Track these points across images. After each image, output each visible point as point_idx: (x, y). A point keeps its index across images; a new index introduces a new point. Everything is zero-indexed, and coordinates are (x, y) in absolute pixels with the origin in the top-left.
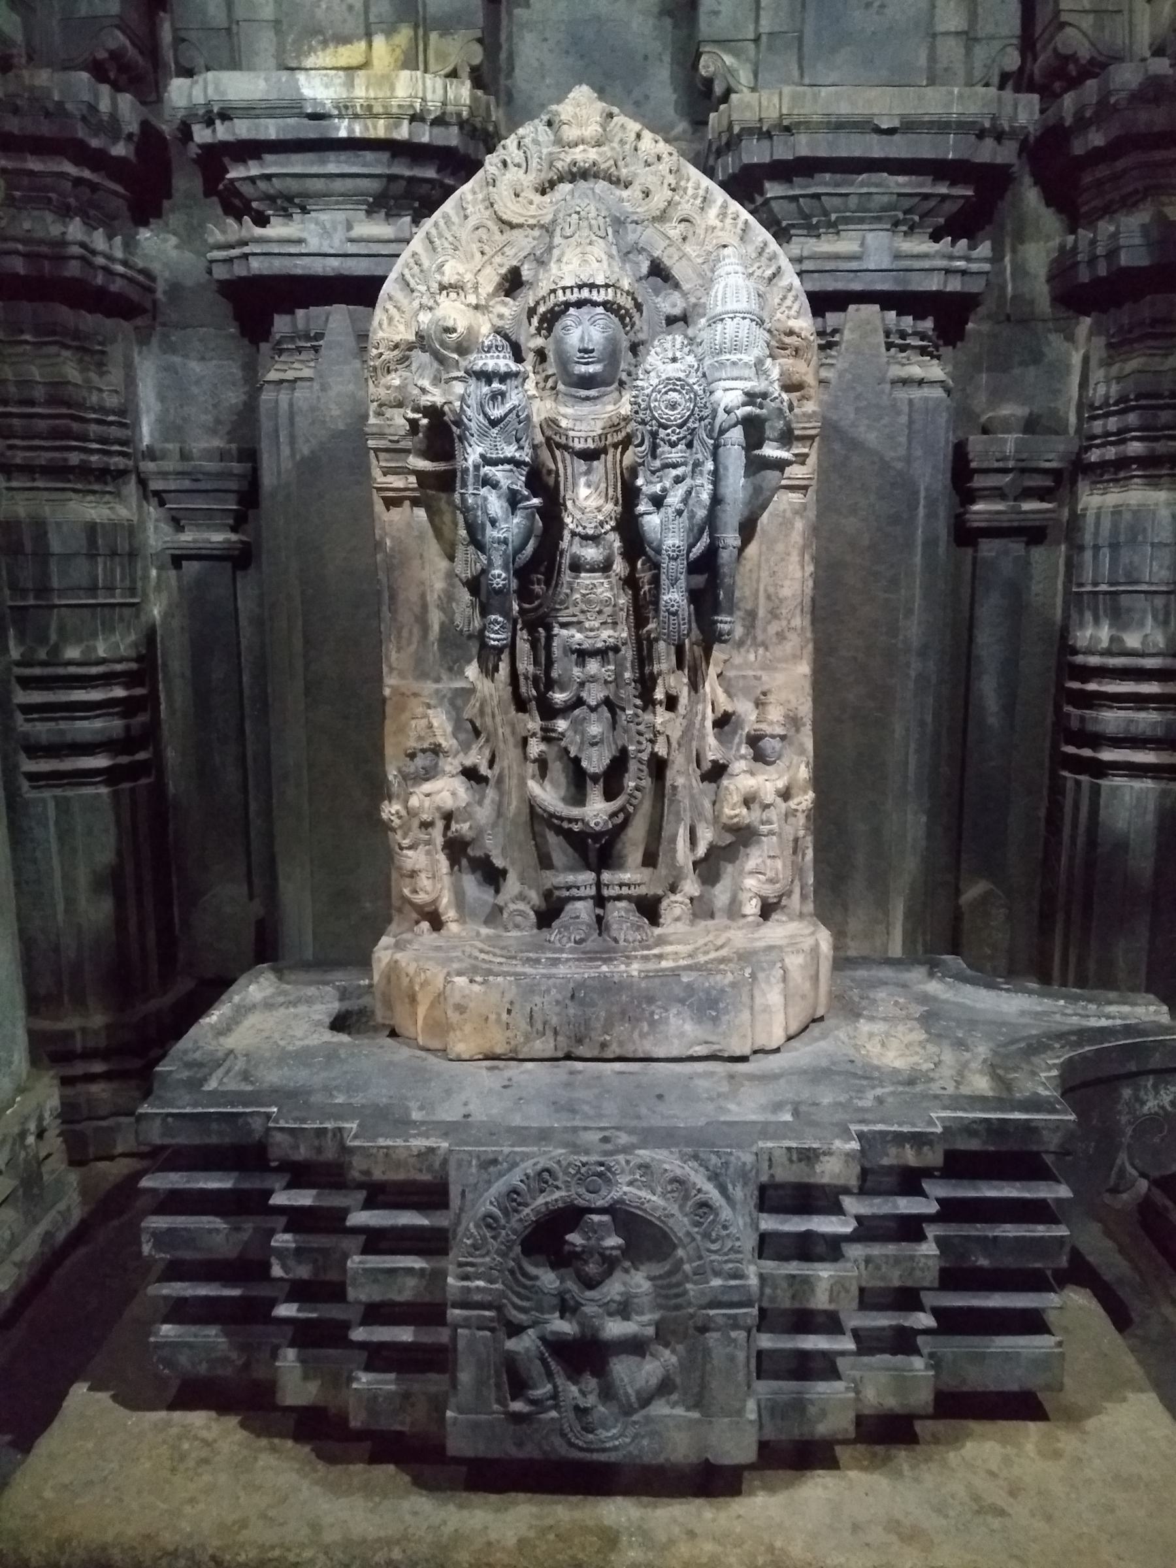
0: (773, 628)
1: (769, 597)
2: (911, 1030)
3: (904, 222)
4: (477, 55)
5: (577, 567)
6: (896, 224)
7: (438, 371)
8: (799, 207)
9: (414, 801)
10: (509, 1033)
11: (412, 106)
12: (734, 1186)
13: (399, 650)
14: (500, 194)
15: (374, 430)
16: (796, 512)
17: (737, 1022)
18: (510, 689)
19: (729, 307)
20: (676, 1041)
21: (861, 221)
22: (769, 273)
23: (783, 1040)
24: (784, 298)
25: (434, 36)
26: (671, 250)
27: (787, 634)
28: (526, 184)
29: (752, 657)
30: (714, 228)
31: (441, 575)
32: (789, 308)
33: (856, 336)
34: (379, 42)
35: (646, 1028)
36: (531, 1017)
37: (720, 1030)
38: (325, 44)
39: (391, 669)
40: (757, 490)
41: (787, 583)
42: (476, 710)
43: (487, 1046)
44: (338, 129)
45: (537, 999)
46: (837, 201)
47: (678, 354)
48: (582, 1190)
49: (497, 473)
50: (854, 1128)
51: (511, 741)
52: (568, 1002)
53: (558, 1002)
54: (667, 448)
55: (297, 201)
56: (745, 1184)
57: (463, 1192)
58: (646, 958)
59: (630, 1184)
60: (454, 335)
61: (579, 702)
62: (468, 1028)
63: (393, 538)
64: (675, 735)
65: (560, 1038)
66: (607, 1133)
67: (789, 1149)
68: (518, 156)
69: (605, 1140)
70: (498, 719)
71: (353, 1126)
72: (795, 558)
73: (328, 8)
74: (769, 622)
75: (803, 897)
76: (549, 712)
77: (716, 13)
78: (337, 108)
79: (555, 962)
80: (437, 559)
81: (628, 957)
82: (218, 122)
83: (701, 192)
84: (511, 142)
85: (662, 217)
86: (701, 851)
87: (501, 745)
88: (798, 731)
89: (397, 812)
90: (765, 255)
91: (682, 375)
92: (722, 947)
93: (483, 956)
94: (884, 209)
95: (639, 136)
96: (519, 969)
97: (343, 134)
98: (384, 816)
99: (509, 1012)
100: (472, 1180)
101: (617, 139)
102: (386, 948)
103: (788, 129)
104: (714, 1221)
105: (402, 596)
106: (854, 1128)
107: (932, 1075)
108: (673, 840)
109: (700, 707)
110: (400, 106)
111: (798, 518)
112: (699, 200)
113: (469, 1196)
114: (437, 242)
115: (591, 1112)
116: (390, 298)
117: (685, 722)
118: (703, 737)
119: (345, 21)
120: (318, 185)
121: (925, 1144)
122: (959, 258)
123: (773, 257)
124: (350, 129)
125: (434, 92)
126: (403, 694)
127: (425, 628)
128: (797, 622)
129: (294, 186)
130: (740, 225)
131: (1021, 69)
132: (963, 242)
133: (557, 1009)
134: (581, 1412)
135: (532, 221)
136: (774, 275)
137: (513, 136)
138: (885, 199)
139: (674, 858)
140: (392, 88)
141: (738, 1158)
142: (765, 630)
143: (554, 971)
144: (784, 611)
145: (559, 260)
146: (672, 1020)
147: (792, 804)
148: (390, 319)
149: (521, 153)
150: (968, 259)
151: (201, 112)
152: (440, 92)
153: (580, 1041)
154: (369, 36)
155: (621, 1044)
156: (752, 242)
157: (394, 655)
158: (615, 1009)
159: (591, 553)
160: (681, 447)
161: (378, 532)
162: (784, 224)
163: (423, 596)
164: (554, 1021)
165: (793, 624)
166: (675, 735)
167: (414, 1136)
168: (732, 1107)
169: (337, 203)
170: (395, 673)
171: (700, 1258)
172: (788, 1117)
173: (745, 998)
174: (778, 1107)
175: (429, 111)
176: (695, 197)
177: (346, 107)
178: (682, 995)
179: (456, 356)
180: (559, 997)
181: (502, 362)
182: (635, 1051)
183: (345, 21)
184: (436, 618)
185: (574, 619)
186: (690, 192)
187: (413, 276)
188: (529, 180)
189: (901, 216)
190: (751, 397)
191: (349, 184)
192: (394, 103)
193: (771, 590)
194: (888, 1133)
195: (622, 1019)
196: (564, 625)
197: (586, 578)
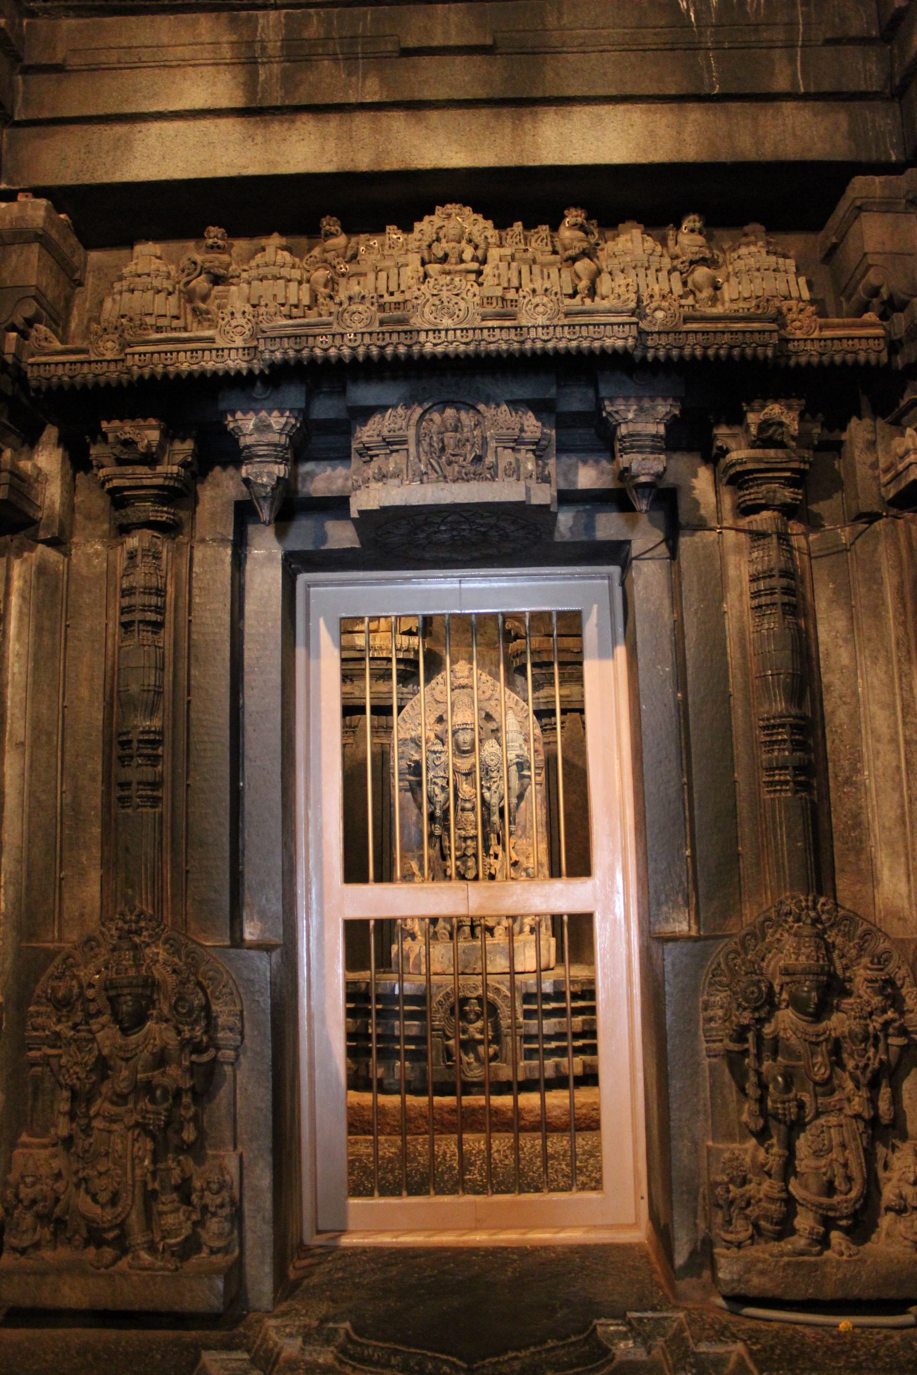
5: (463, 810)
40: (522, 785)
49: (438, 781)
64: (498, 868)
85: (489, 699)
103: (539, 652)
134: (469, 1064)
153: (466, 967)
159: (468, 805)
166: (498, 868)
181: (439, 748)
190: (518, 756)
197: (466, 813)
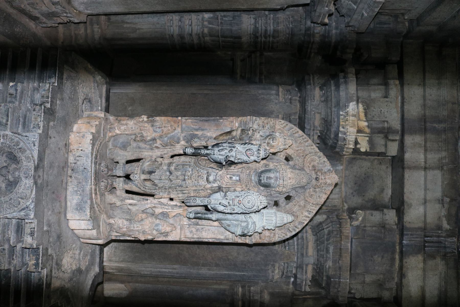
0: (194, 230)
1: (202, 228)
2: (76, 265)
3: (317, 267)
4: (363, 150)
6: (317, 265)
7: (264, 137)
8: (322, 238)
9: (146, 125)
10: (76, 150)
11: (348, 132)
12: (24, 212)
13: (192, 122)
14: (312, 156)
15: (252, 118)
16: (226, 237)
17: (76, 216)
18: (177, 153)
19: (278, 219)
20: (71, 198)
21: (318, 256)
22: (291, 229)
23: (71, 228)
24: (284, 234)
25: (367, 138)
26: (297, 202)
27: (192, 234)
28: (314, 163)
29: (185, 223)
30: (302, 214)
31: (211, 135)
32: (281, 235)
33: (286, 254)
34: (366, 124)
35: (75, 189)
36: (80, 156)
37: (74, 211)
38: (365, 109)
39: (186, 120)
41: (206, 234)
42: (172, 143)
43: (73, 144)
44: (342, 112)
45: (85, 158)
46: (322, 248)
47: (262, 204)
48: (24, 170)
50: (41, 247)
51: (162, 153)
52: (83, 167)
53: (84, 164)
54: (237, 200)
55: (326, 99)
56: (25, 215)
57: (27, 136)
58: (96, 190)
59: (26, 184)
60: (272, 142)
61: (171, 173)
62: (78, 138)
63: (222, 122)
65: (74, 164)
66: (41, 177)
67: (34, 228)
68: (322, 161)
69: (39, 177)
70: (169, 149)
71: (48, 106)
72: (213, 236)
73: (373, 111)
74: (195, 228)
75: (116, 236)
76: (170, 164)
77: (372, 215)
78: (347, 112)
79: (95, 163)
80: (216, 134)
81: (96, 184)
82: (344, 80)
83: (312, 211)
84: (326, 159)
86: (130, 207)
87: (162, 150)
88: (164, 236)
89: (143, 120)
90: (295, 228)
91: (256, 205)
92: (100, 212)
93: (100, 143)
94: (320, 261)
95: (326, 194)
96: (94, 153)
97: (341, 113)
98: (143, 116)
99: (82, 150)
100: (30, 139)
101: (326, 188)
102: (105, 115)
104: (14, 206)
105: (206, 124)
106: (41, 247)
107: (60, 270)
108: (133, 199)
109: (170, 208)
110: (347, 129)
111: (224, 237)
112: (310, 210)
113: (25, 138)
114: (301, 138)
115: (49, 173)
116: (287, 125)
117: (166, 203)
118: (161, 208)
119: (370, 115)
120: (329, 105)
121: (36, 266)
122: (305, 282)
123: (295, 230)
124: (342, 115)
125: (351, 138)
126: (179, 123)
127: (197, 130)
128: (195, 236)
129: (329, 99)
130: (303, 221)
131: (356, 298)
132: (310, 284)
133: (82, 164)
135: (305, 164)
136: (290, 231)
137: (327, 160)
138: (322, 262)
139: (127, 199)
140: (352, 127)
141: (32, 214)
142: (193, 227)
143: (93, 163)
144: (198, 233)
145: (292, 172)
146: (77, 197)
147: (141, 234)
148: (282, 124)
149: (322, 162)
150: (305, 285)
151: (346, 76)
152: (351, 140)
153: (72, 170)
154: (367, 121)
155: (71, 182)
156: (299, 224)
157: (190, 121)
158: (81, 180)
160: (238, 204)
161: (225, 117)
162: (318, 234)
163: (206, 130)
164: (78, 163)
165: (195, 235)
167: (44, 123)
168: (50, 213)
169: (325, 110)
170: (185, 120)
171: (5, 202)
172: (45, 228)
173: (82, 218)
174: (49, 225)
175: (346, 136)
176: (311, 209)
177: (347, 114)
178: (84, 200)
179: (267, 142)
180: (85, 165)
182: (69, 186)
183: (370, 115)
184: (199, 133)
185: (194, 173)
186: (312, 208)
187: (292, 131)
188: (315, 163)
189: (319, 266)
191: (330, 114)
192: (349, 127)
193: (204, 229)
194: (39, 256)
195: (78, 182)
196: (192, 170)
